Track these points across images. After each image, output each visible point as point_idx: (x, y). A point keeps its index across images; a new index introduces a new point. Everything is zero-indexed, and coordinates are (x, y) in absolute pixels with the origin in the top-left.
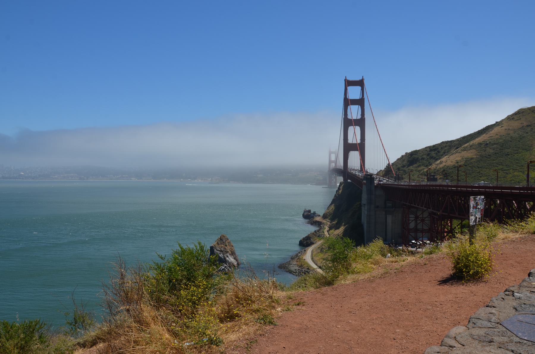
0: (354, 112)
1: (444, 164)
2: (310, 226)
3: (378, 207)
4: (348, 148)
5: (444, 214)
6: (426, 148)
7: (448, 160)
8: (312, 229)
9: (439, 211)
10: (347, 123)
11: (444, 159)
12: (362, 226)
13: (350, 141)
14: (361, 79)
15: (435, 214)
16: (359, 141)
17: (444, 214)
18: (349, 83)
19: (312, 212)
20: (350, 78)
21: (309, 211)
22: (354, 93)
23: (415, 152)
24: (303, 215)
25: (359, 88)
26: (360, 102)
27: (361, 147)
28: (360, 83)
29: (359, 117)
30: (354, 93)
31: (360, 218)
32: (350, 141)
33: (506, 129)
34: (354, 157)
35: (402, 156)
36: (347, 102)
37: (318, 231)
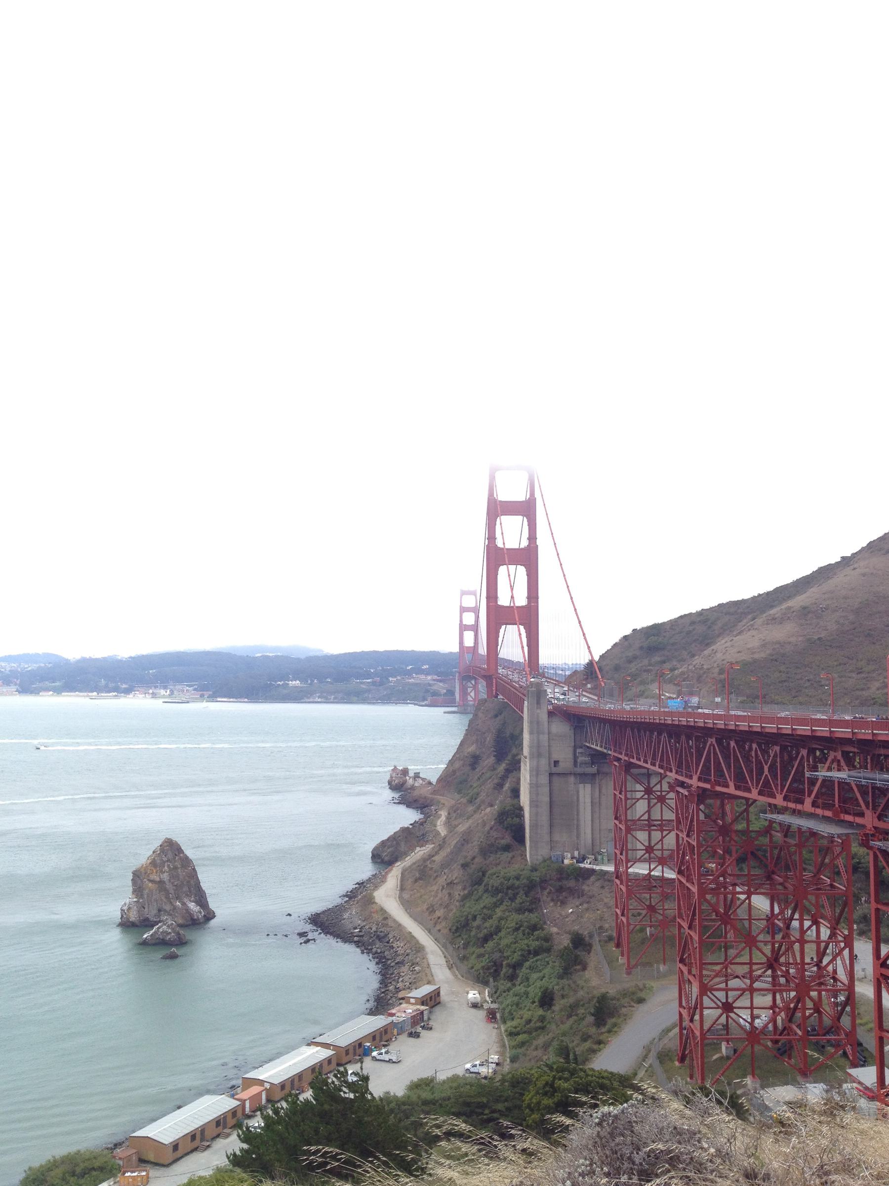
2: (402, 809)
3: (556, 763)
4: (499, 616)
5: (701, 785)
6: (681, 617)
7: (729, 650)
8: (408, 817)
9: (691, 777)
10: (496, 557)
12: (521, 809)
13: (504, 600)
15: (682, 784)
16: (521, 600)
17: (701, 785)
19: (411, 774)
21: (405, 772)
23: (656, 629)
24: (390, 783)
27: (528, 617)
29: (525, 543)
31: (516, 793)
33: (864, 575)
35: (625, 638)
37: (422, 824)
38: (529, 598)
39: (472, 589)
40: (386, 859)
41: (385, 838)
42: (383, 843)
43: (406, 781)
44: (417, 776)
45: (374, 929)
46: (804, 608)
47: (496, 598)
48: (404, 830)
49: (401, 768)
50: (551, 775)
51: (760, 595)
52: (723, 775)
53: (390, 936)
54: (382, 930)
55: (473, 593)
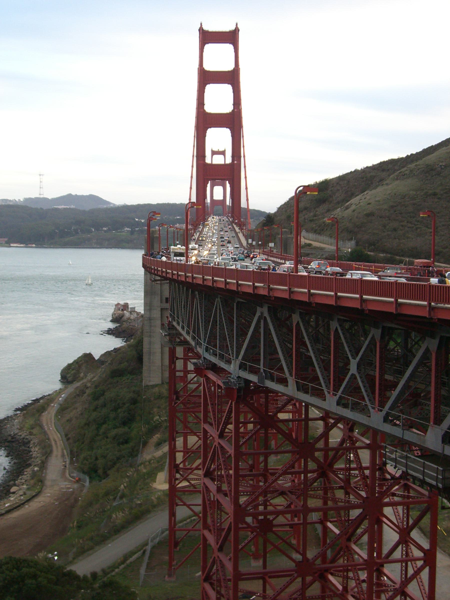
0: (219, 99)
1: (353, 207)
11: (354, 200)
14: (233, 28)
18: (207, 37)
20: (210, 27)
21: (126, 306)
22: (219, 58)
25: (229, 47)
26: (232, 78)
27: (231, 174)
28: (231, 37)
30: (219, 58)
32: (208, 160)
34: (218, 192)
36: (206, 78)
38: (233, 157)
39: (222, 149)
40: (70, 379)
41: (71, 361)
42: (69, 366)
43: (123, 316)
44: (133, 311)
45: (23, 436)
46: (428, 166)
47: (204, 156)
48: (88, 357)
49: (122, 303)
50: (162, 309)
51: (408, 156)
52: (174, 313)
53: (32, 442)
54: (27, 437)
55: (223, 153)
